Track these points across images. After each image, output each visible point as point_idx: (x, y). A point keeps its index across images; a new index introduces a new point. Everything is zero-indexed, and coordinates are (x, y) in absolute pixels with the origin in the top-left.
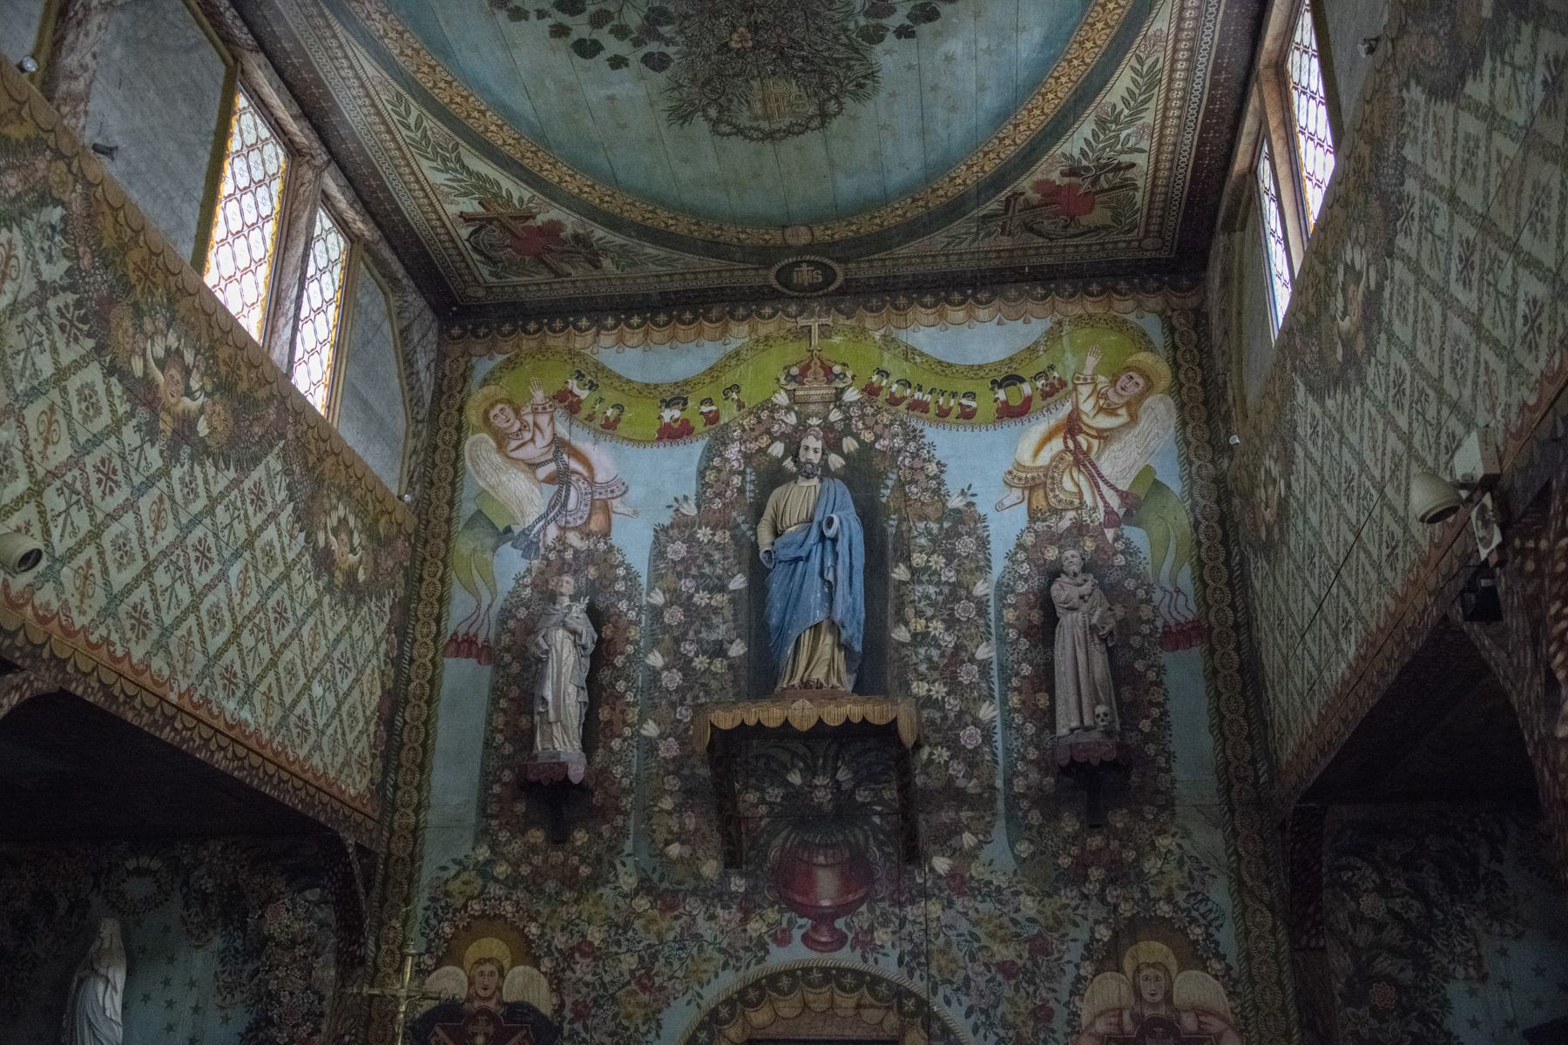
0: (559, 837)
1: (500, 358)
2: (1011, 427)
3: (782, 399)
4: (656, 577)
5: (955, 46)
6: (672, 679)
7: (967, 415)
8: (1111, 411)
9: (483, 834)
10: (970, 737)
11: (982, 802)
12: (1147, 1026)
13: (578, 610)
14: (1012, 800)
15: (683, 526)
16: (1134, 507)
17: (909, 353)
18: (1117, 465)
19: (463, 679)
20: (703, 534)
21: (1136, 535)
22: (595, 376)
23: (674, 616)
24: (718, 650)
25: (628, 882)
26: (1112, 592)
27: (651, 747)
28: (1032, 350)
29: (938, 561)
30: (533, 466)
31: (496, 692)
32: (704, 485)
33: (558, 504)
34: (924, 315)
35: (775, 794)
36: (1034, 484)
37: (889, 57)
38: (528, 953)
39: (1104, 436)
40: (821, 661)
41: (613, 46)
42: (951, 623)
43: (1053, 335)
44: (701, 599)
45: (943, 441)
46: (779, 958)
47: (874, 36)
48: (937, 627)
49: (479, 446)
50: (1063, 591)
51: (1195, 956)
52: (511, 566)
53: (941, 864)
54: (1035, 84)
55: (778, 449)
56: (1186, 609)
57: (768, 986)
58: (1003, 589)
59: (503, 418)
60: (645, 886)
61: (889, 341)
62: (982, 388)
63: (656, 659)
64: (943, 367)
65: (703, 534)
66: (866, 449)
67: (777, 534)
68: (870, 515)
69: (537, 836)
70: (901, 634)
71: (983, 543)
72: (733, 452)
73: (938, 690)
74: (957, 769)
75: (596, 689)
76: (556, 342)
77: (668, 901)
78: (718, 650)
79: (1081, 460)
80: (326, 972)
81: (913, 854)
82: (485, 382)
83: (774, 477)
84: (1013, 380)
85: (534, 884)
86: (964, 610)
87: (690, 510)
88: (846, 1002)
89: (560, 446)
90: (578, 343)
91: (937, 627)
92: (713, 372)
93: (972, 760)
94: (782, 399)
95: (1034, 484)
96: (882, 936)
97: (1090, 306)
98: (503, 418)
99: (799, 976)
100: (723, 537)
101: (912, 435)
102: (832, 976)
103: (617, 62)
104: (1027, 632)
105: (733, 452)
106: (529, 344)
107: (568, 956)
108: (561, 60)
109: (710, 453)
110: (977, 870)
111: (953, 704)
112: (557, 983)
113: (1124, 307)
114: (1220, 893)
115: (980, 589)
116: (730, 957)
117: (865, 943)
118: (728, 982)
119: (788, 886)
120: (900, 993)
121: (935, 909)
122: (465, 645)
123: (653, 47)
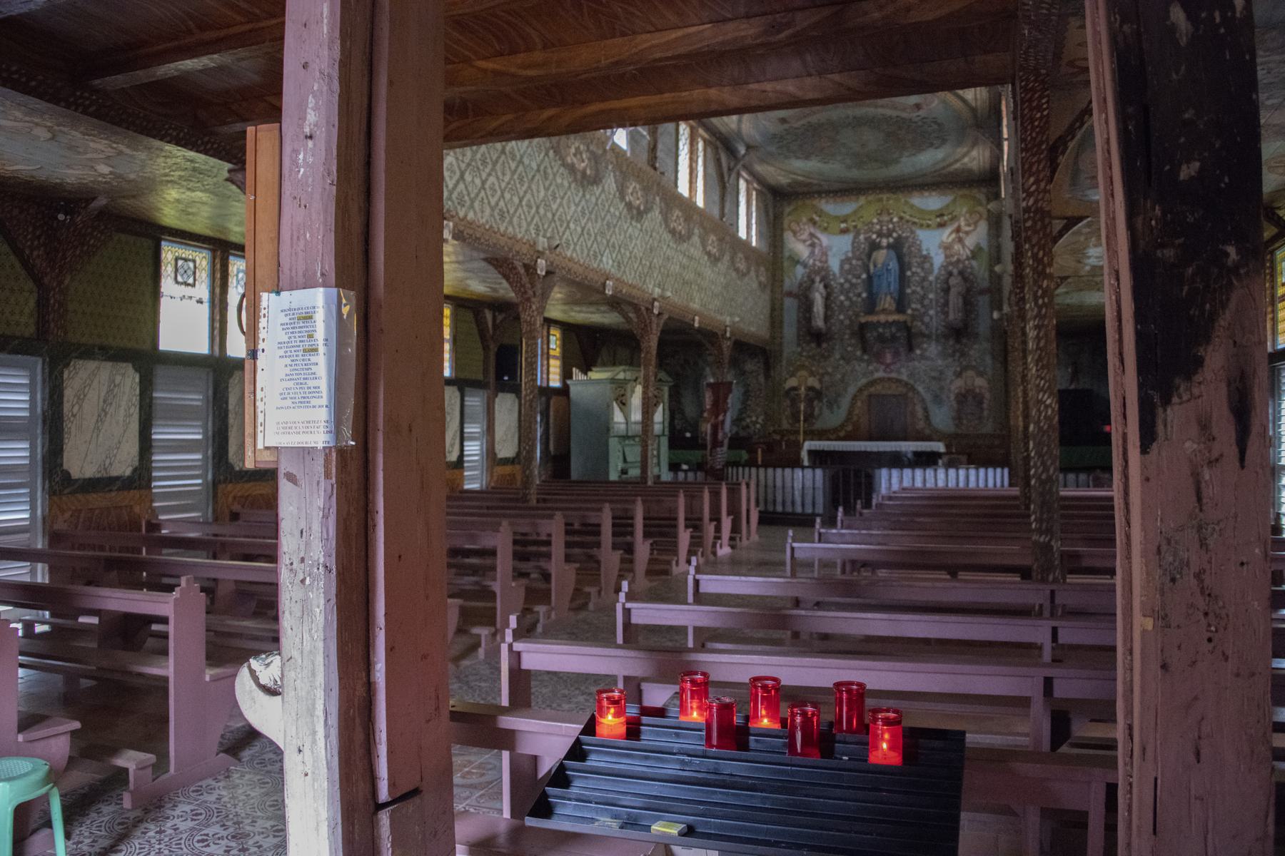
0: (819, 345)
1: (792, 207)
2: (940, 230)
3: (875, 221)
4: (841, 274)
6: (847, 303)
7: (928, 226)
8: (969, 225)
9: (799, 345)
10: (927, 319)
11: (929, 337)
12: (968, 391)
13: (821, 286)
14: (937, 336)
15: (848, 260)
16: (975, 254)
17: (912, 206)
18: (970, 242)
19: (790, 304)
20: (854, 262)
21: (974, 263)
22: (821, 213)
23: (847, 286)
24: (859, 295)
25: (838, 356)
26: (965, 279)
27: (842, 322)
28: (948, 206)
29: (919, 270)
30: (804, 241)
31: (799, 307)
32: (853, 247)
33: (812, 253)
34: (916, 193)
35: (875, 334)
36: (947, 248)
37: (904, 159)
38: (812, 374)
39: (967, 233)
40: (887, 302)
42: (923, 288)
43: (954, 201)
44: (854, 281)
45: (922, 235)
46: (877, 375)
48: (919, 289)
49: (788, 236)
50: (953, 281)
51: (980, 374)
52: (800, 271)
53: (918, 352)
54: (944, 160)
55: (874, 236)
56: (986, 284)
57: (872, 383)
58: (937, 278)
59: (794, 226)
60: (843, 358)
61: (906, 203)
62: (933, 217)
63: (842, 298)
64: (922, 211)
65: (854, 262)
66: (900, 236)
67: (875, 266)
68: (900, 258)
69: (813, 345)
70: (909, 291)
71: (932, 265)
72: (862, 237)
73: (919, 306)
74: (923, 327)
75: (827, 307)
76: (808, 202)
77: (848, 362)
78: (859, 295)
79: (960, 240)
80: (762, 379)
81: (911, 349)
82: (789, 214)
83: (874, 246)
84: (942, 215)
85: (812, 358)
86: (926, 284)
87: (850, 255)
88: (894, 386)
89: (812, 235)
90: (816, 202)
91: (919, 289)
92: (855, 212)
93: (927, 326)
94: (875, 221)
95: (947, 248)
96: (903, 370)
97: (965, 191)
98: (794, 226)
99: (881, 380)
100: (860, 263)
101: (912, 232)
102: (889, 379)
104: (943, 290)
105: (862, 237)
106: (800, 203)
107: (823, 375)
108: (819, 165)
109: (856, 237)
110: (927, 354)
111: (923, 310)
112: (821, 381)
113: (975, 191)
114: (988, 360)
115: (931, 278)
116: (864, 375)
117: (899, 372)
118: (864, 381)
119: (878, 357)
120: (906, 384)
121: (916, 363)
122: (790, 294)
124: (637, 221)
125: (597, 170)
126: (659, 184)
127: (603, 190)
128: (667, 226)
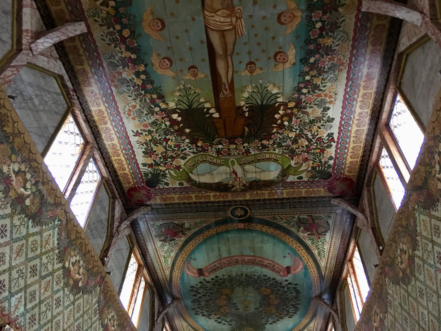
5: (278, 326)
37: (268, 326)
41: (224, 322)
47: (266, 324)
103: (224, 324)
108: (216, 324)
123: (230, 323)
124: (71, 291)
125: (40, 210)
126: (103, 278)
127: (40, 233)
128: (101, 318)
